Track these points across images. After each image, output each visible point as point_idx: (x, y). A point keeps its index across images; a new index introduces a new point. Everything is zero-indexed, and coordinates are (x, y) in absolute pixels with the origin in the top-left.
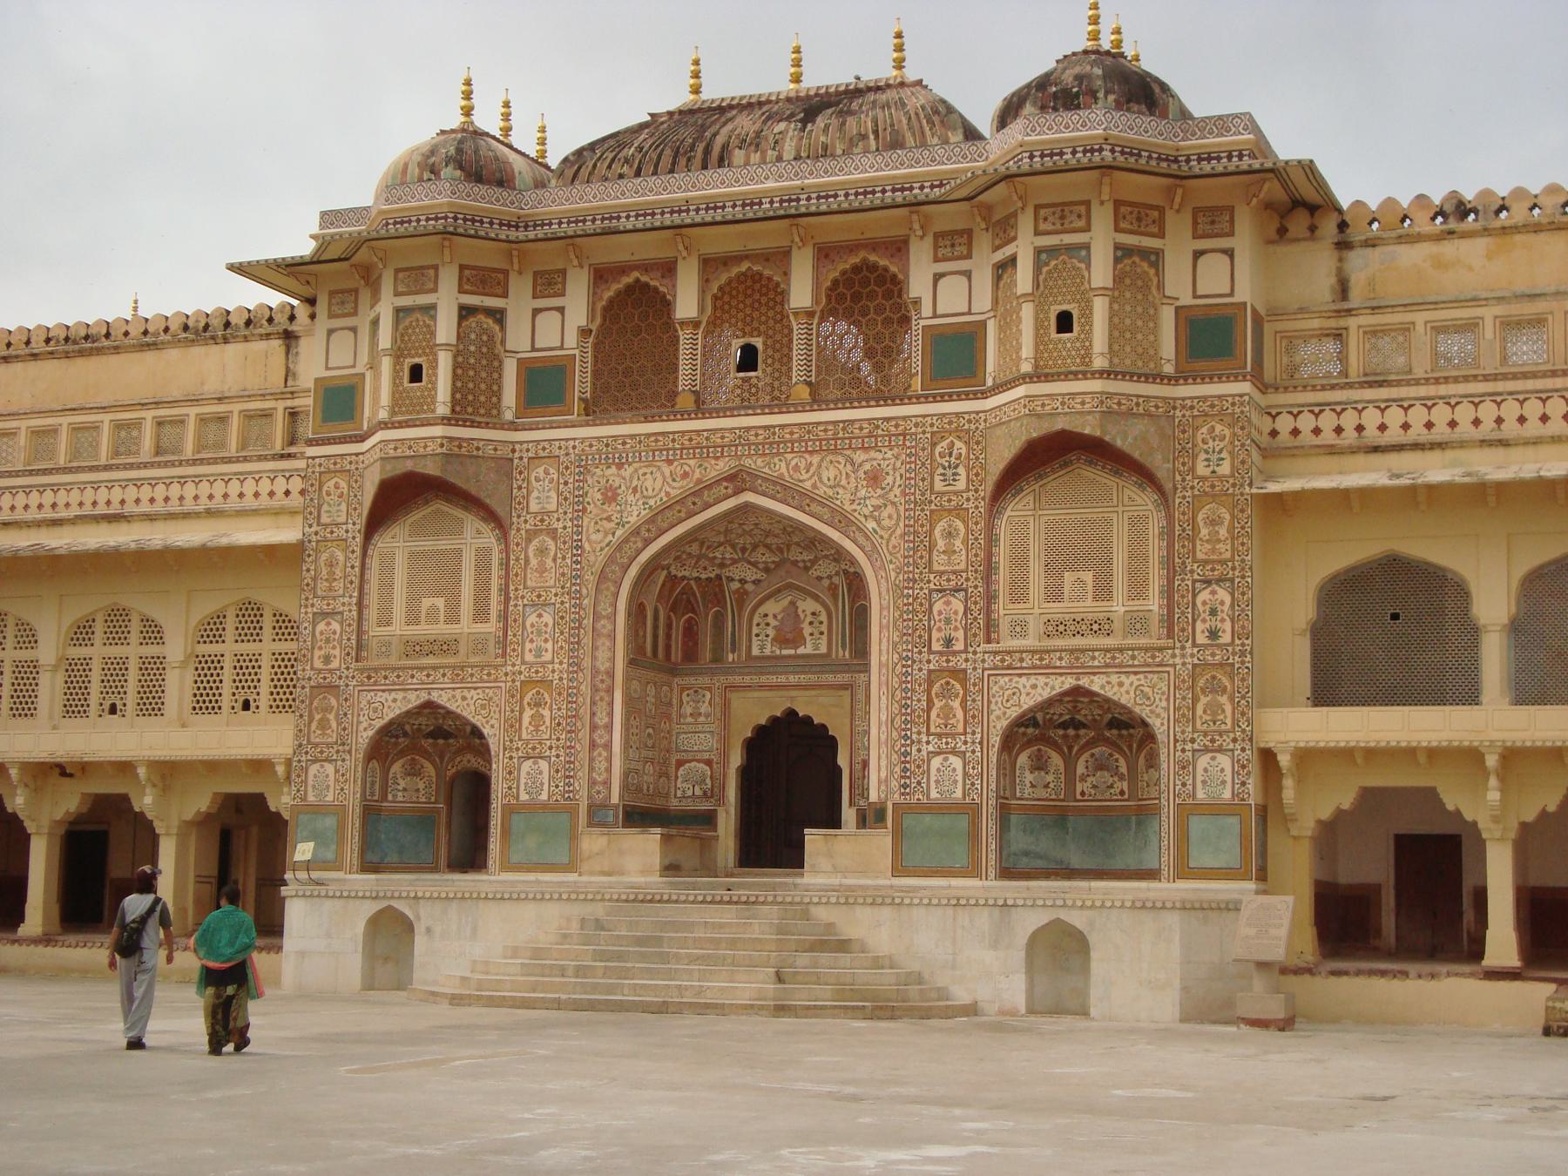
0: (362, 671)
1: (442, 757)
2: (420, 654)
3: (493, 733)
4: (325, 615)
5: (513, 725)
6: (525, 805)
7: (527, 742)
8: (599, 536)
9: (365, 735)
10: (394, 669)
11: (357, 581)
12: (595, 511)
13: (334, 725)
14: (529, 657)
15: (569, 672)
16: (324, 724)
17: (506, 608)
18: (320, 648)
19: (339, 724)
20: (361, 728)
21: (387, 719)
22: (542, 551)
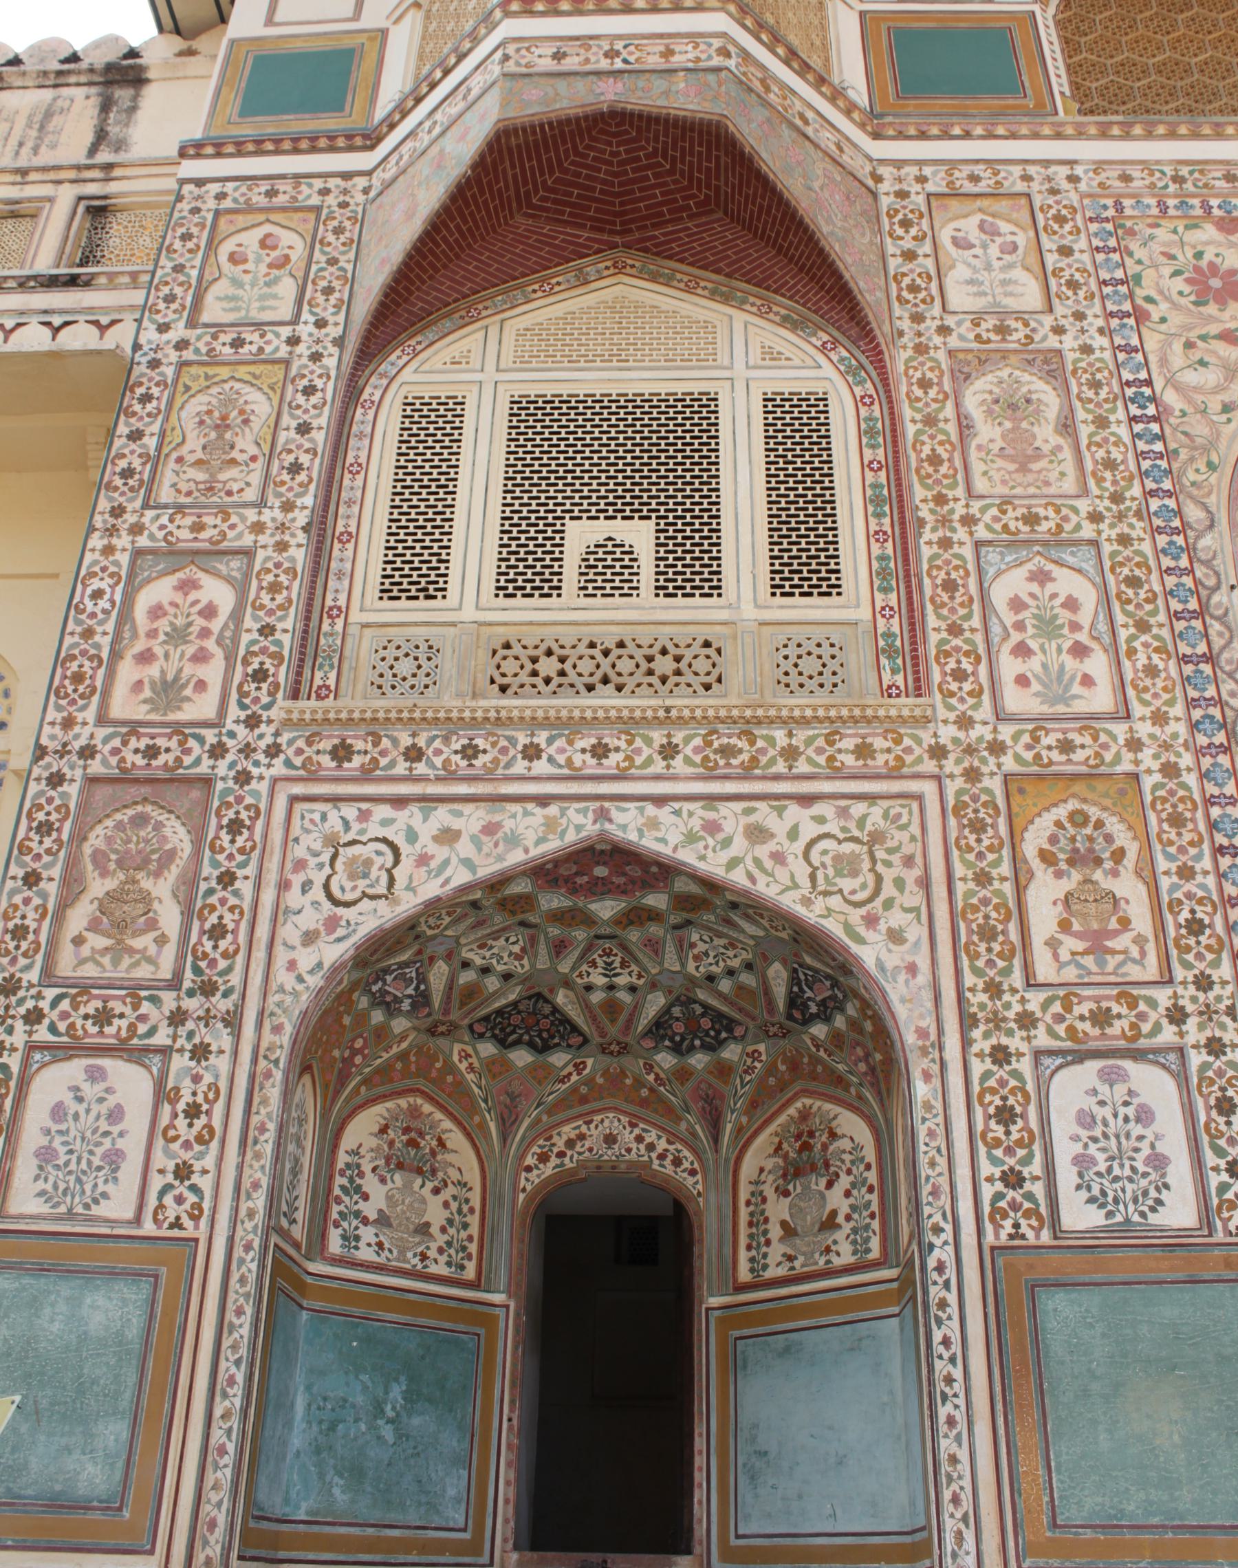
0: (313, 729)
1: (507, 1126)
2: (559, 681)
3: (899, 963)
4: (174, 556)
5: (992, 933)
6: (1088, 1245)
7: (1068, 995)
8: (1210, 377)
9: (306, 958)
10: (448, 725)
11: (315, 467)
12: (1176, 319)
13: (169, 917)
14: (1014, 700)
15: (1199, 752)
16: (122, 917)
17: (906, 553)
18: (145, 657)
19: (188, 914)
20: (290, 932)
21: (407, 904)
22: (1013, 407)
